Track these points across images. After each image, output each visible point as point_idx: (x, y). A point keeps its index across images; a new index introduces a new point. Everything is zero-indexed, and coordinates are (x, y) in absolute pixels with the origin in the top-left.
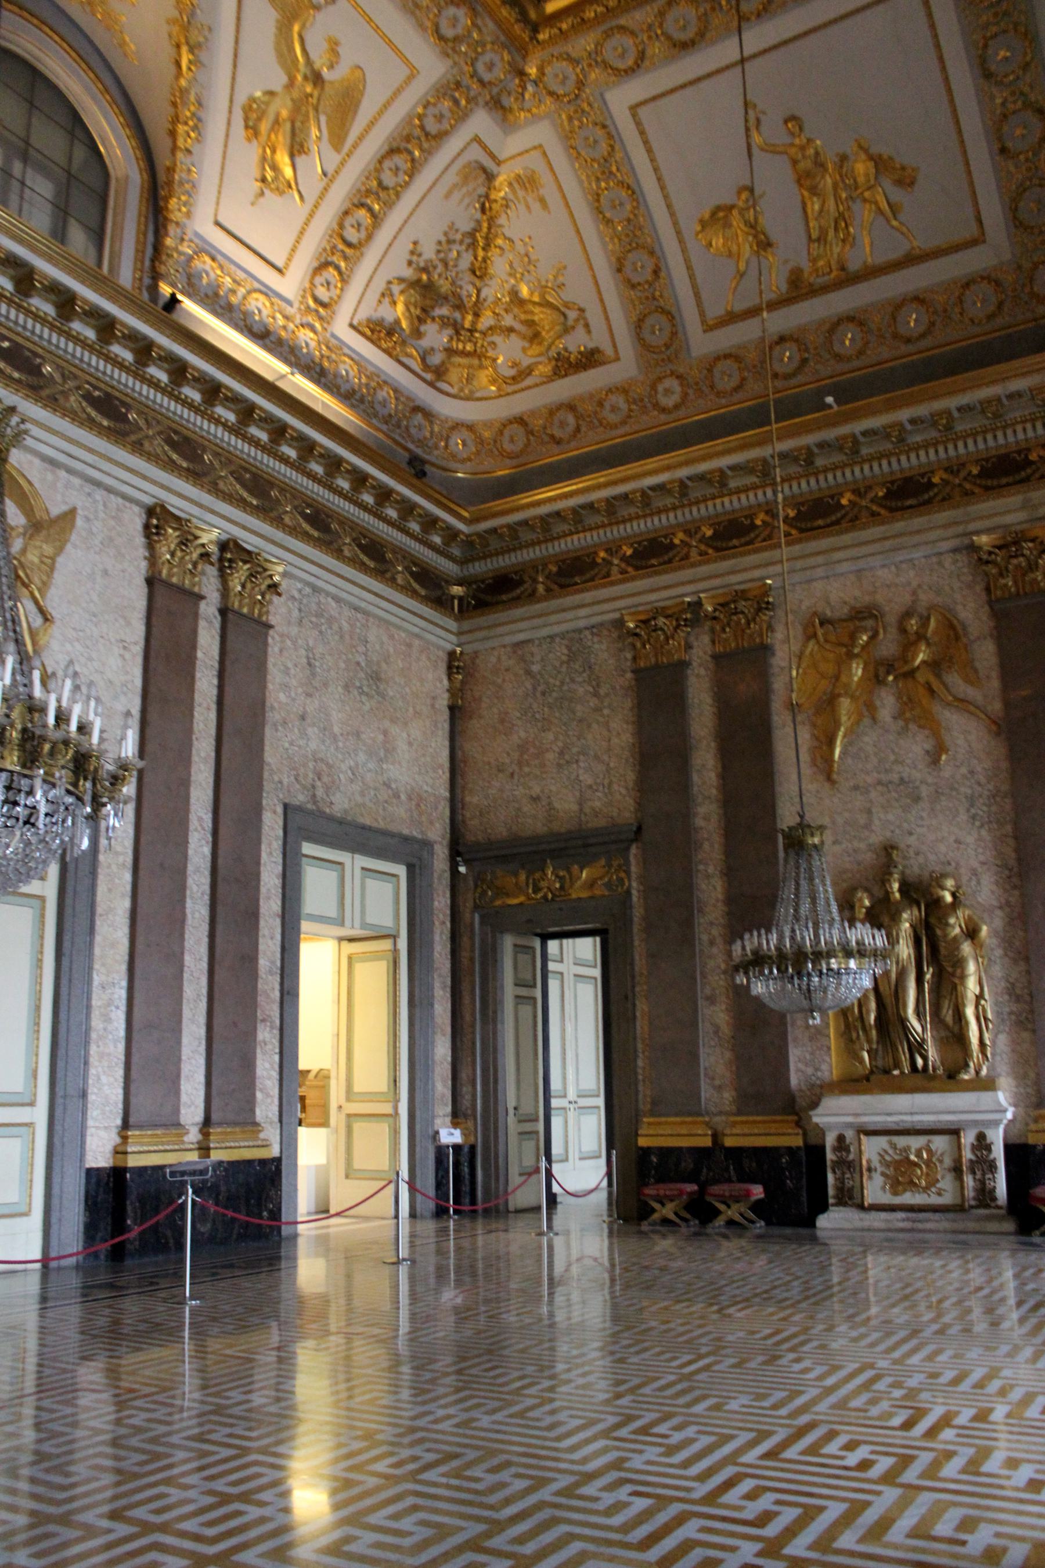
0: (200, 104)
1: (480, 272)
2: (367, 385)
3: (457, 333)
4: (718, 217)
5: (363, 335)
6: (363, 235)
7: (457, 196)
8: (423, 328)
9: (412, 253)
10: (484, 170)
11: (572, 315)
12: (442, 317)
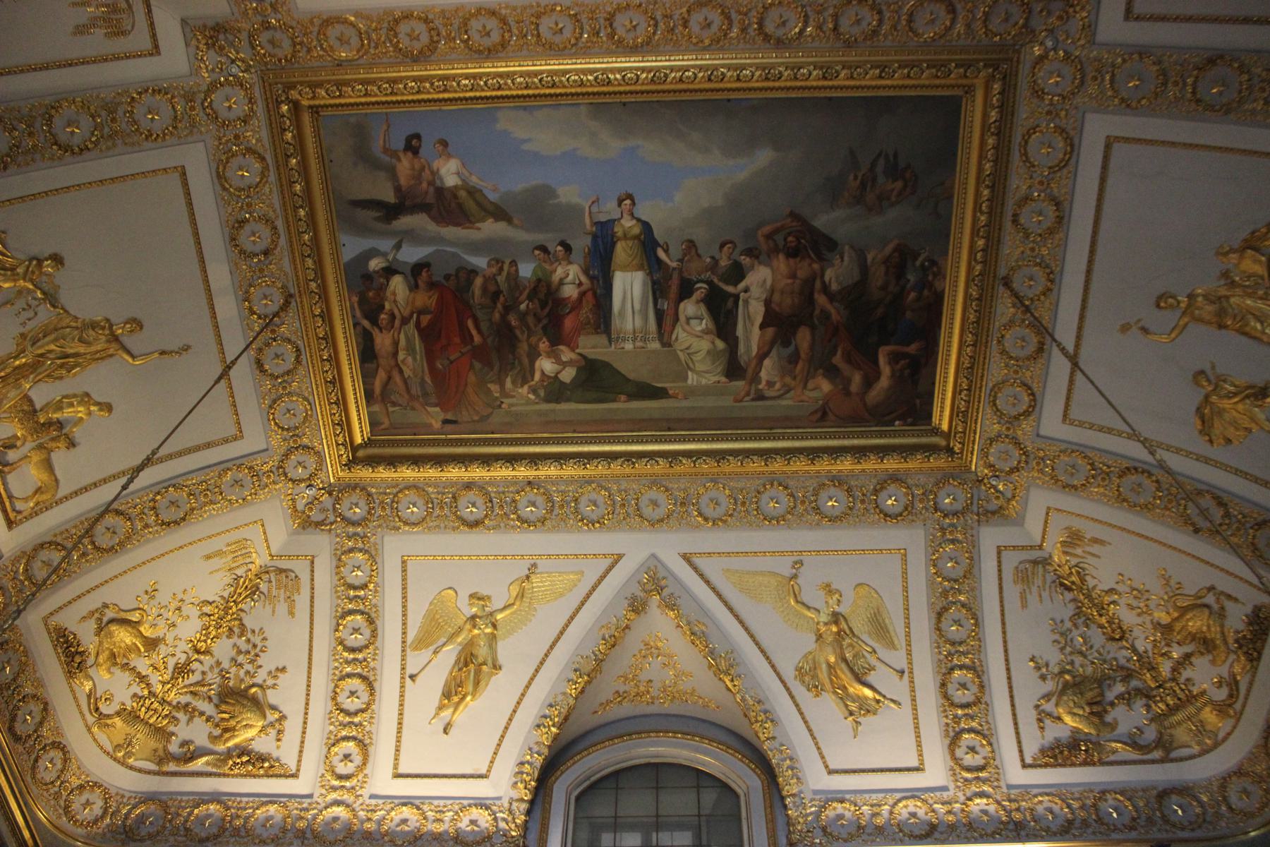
0: (759, 702)
1: (1119, 634)
2: (1082, 807)
3: (1148, 697)
4: (1206, 419)
5: (1046, 765)
6: (974, 689)
7: (1033, 599)
8: (1108, 719)
9: (1038, 668)
10: (1035, 562)
11: (1210, 599)
12: (1120, 697)
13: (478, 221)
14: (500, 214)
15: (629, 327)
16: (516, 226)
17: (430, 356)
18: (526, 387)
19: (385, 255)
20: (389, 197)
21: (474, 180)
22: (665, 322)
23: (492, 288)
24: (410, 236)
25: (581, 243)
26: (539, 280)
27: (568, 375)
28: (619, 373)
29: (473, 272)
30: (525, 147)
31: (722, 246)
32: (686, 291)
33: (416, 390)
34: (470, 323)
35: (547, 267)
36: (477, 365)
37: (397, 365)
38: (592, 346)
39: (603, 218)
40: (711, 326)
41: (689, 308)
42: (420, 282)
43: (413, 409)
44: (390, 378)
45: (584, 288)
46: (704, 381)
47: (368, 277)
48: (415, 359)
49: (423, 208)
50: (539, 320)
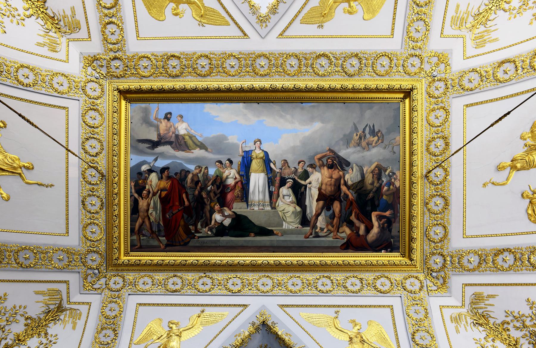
13: (193, 149)
14: (202, 146)
15: (257, 199)
16: (209, 152)
17: (164, 211)
18: (207, 228)
19: (149, 163)
20: (155, 138)
21: (193, 132)
22: (273, 197)
23: (196, 179)
24: (162, 155)
25: (237, 160)
26: (217, 176)
27: (227, 222)
28: (251, 221)
29: (188, 172)
30: (216, 119)
31: (299, 163)
32: (283, 182)
33: (155, 229)
34: (184, 196)
35: (221, 170)
36: (185, 216)
37: (148, 216)
38: (239, 208)
39: (247, 149)
40: (294, 200)
41: (285, 190)
42: (163, 176)
43: (152, 238)
44: (143, 222)
45: (237, 180)
46: (291, 227)
47: (140, 174)
48: (156, 213)
49: (170, 143)
50: (215, 194)
